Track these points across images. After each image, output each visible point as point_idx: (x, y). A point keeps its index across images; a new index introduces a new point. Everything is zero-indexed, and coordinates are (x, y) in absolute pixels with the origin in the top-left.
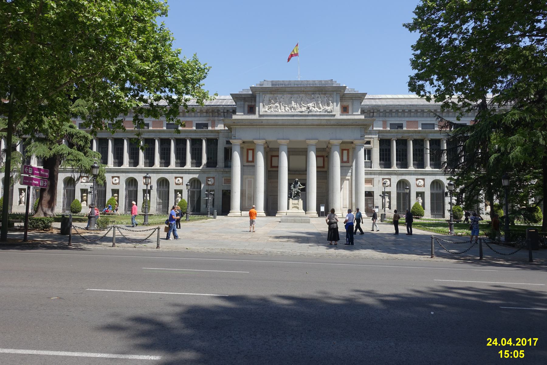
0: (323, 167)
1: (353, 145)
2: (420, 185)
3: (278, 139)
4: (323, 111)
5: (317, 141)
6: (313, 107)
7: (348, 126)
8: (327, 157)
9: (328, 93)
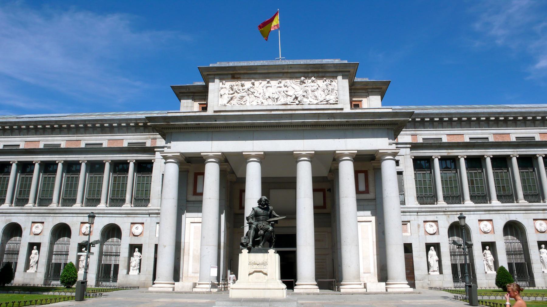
0: (324, 207)
1: (374, 164)
2: (486, 230)
6: (304, 96)
8: (329, 190)
9: (328, 75)
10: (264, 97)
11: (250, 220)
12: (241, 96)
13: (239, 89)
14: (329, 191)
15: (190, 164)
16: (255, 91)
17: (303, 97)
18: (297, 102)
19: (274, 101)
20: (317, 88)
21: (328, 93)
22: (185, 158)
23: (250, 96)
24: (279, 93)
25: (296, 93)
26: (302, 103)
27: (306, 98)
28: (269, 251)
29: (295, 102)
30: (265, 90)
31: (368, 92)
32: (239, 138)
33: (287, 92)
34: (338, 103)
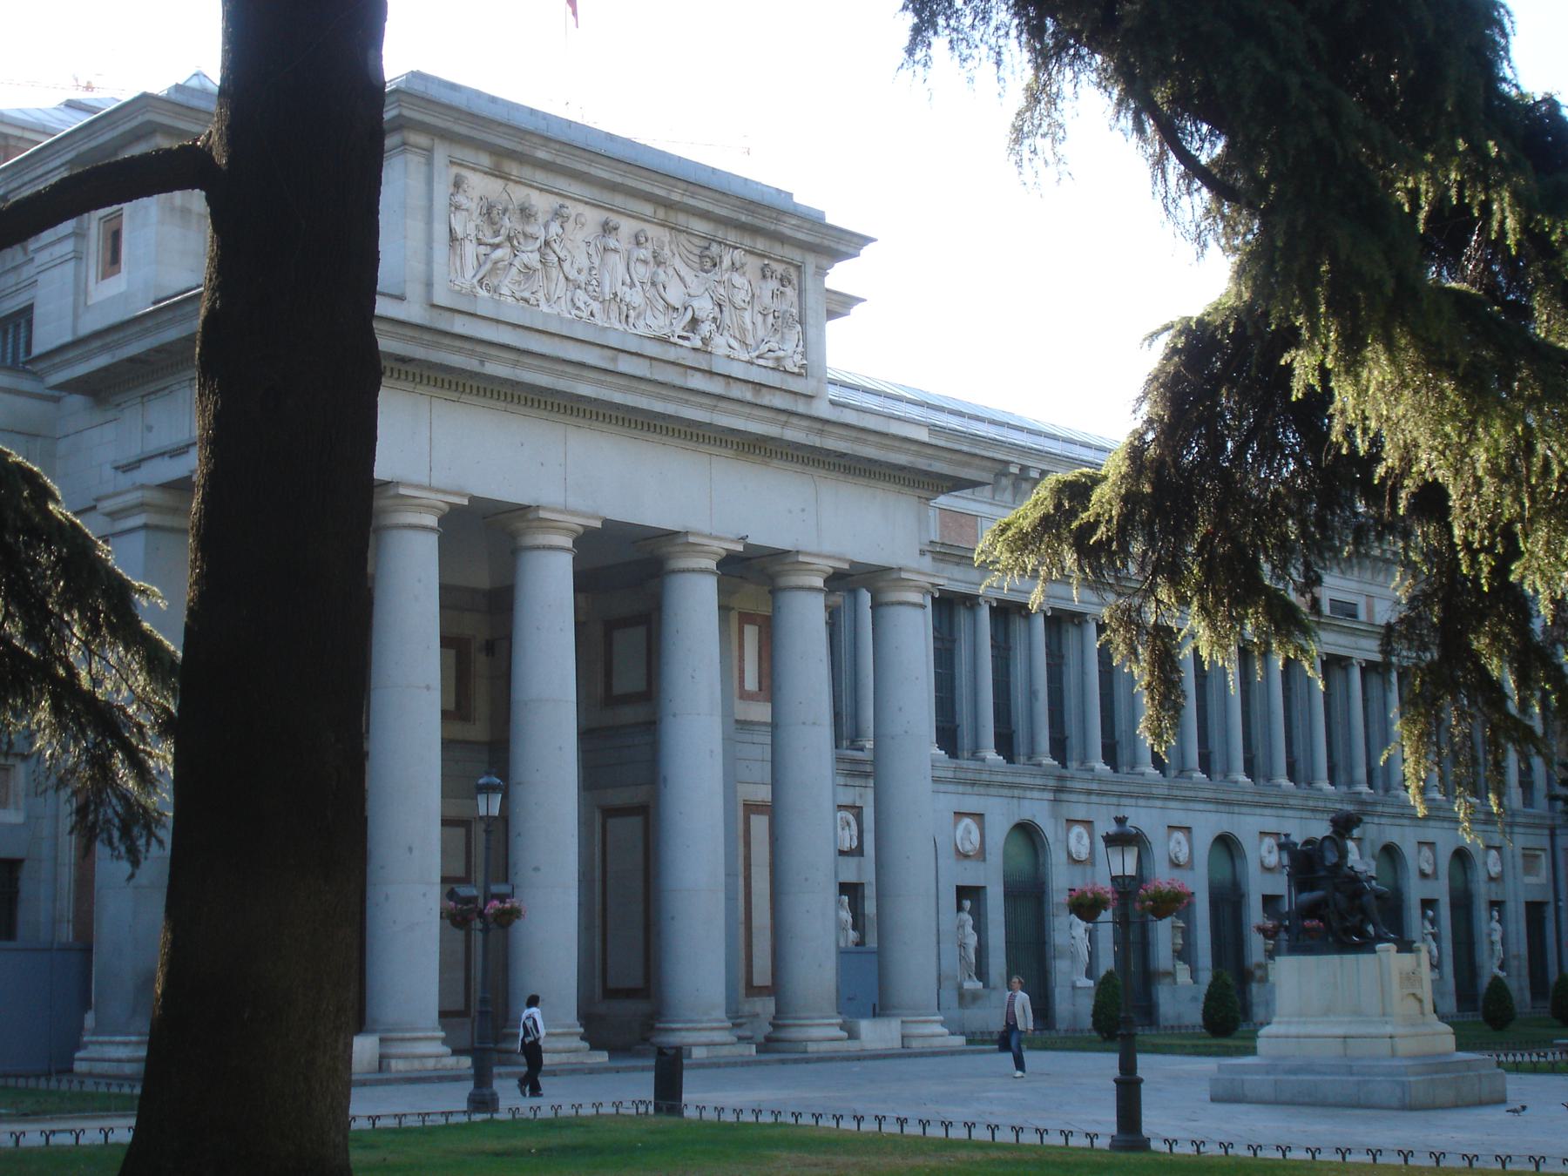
2: (968, 847)
4: (761, 362)
12: (526, 267)
19: (627, 316)
25: (696, 304)
26: (709, 349)
30: (596, 261)
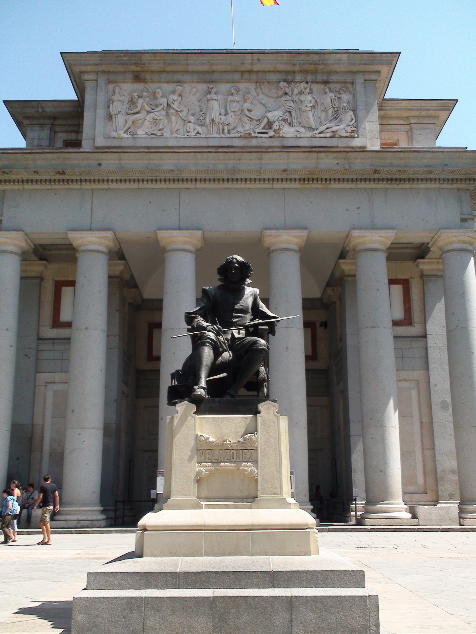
3: (159, 229)
4: (322, 135)
5: (304, 233)
7: (415, 185)
8: (324, 324)
10: (203, 121)
11: (196, 320)
12: (153, 119)
13: (151, 103)
14: (323, 327)
15: (44, 262)
16: (182, 108)
17: (283, 123)
18: (271, 133)
19: (223, 130)
20: (311, 105)
21: (335, 115)
22: (33, 247)
23: (174, 118)
24: (232, 114)
25: (269, 115)
26: (281, 135)
27: (290, 124)
28: (262, 407)
29: (266, 133)
31: (410, 124)
32: (150, 203)
33: (249, 111)
34: (356, 136)
